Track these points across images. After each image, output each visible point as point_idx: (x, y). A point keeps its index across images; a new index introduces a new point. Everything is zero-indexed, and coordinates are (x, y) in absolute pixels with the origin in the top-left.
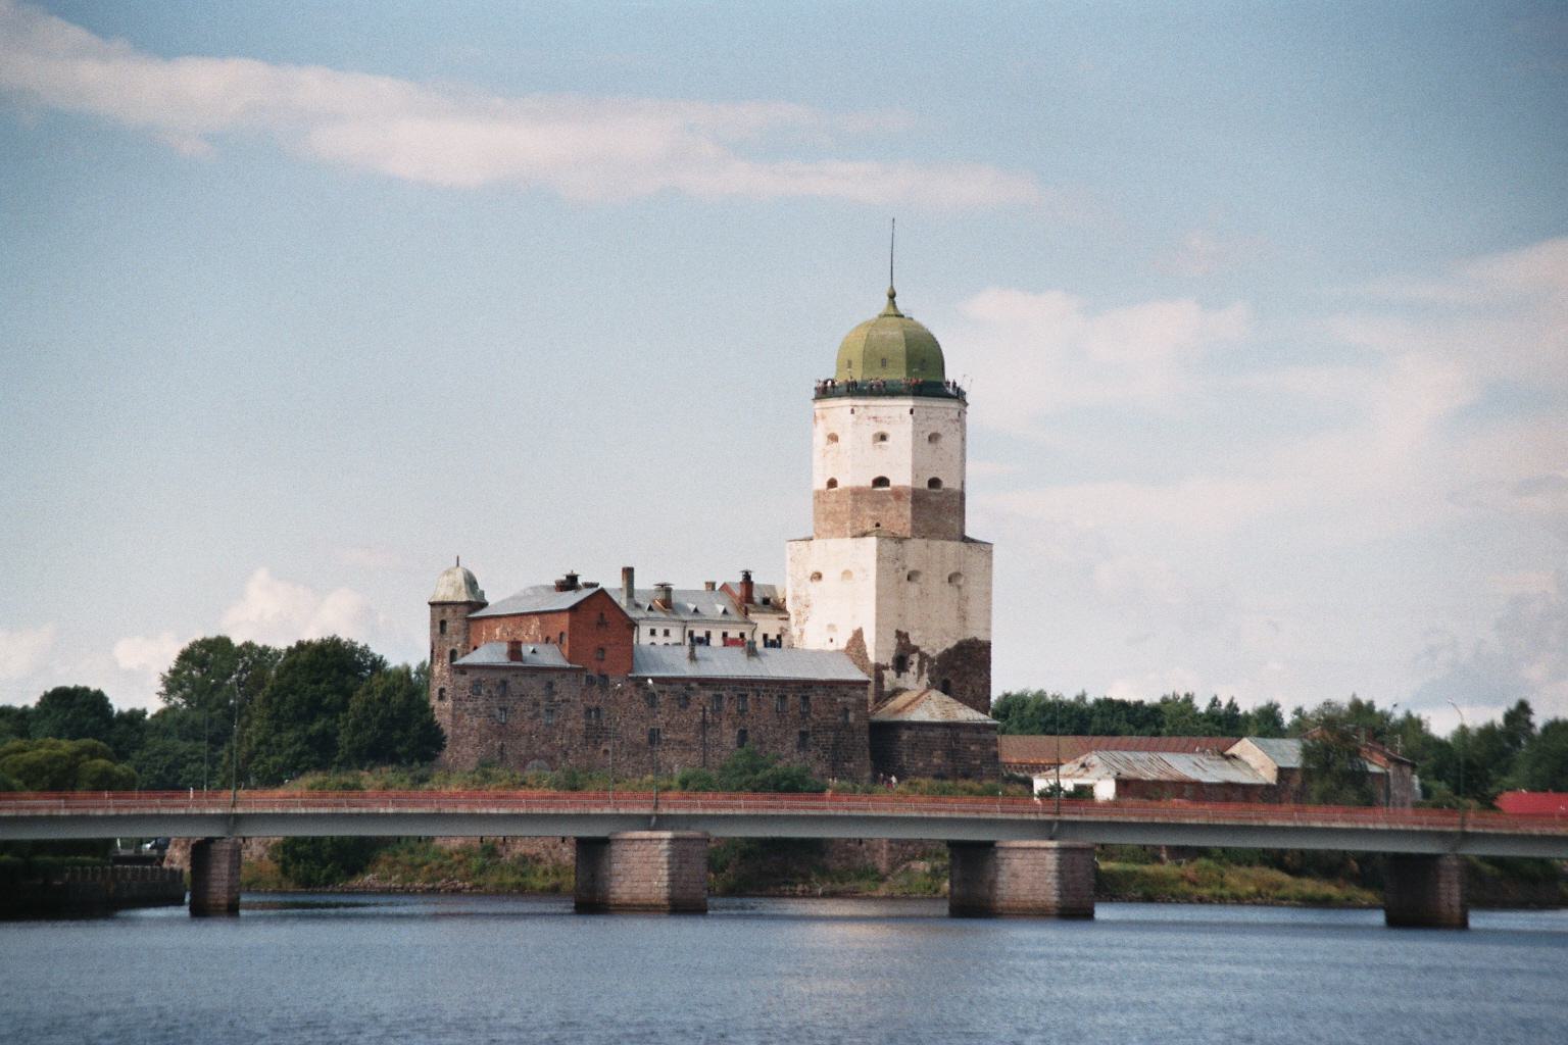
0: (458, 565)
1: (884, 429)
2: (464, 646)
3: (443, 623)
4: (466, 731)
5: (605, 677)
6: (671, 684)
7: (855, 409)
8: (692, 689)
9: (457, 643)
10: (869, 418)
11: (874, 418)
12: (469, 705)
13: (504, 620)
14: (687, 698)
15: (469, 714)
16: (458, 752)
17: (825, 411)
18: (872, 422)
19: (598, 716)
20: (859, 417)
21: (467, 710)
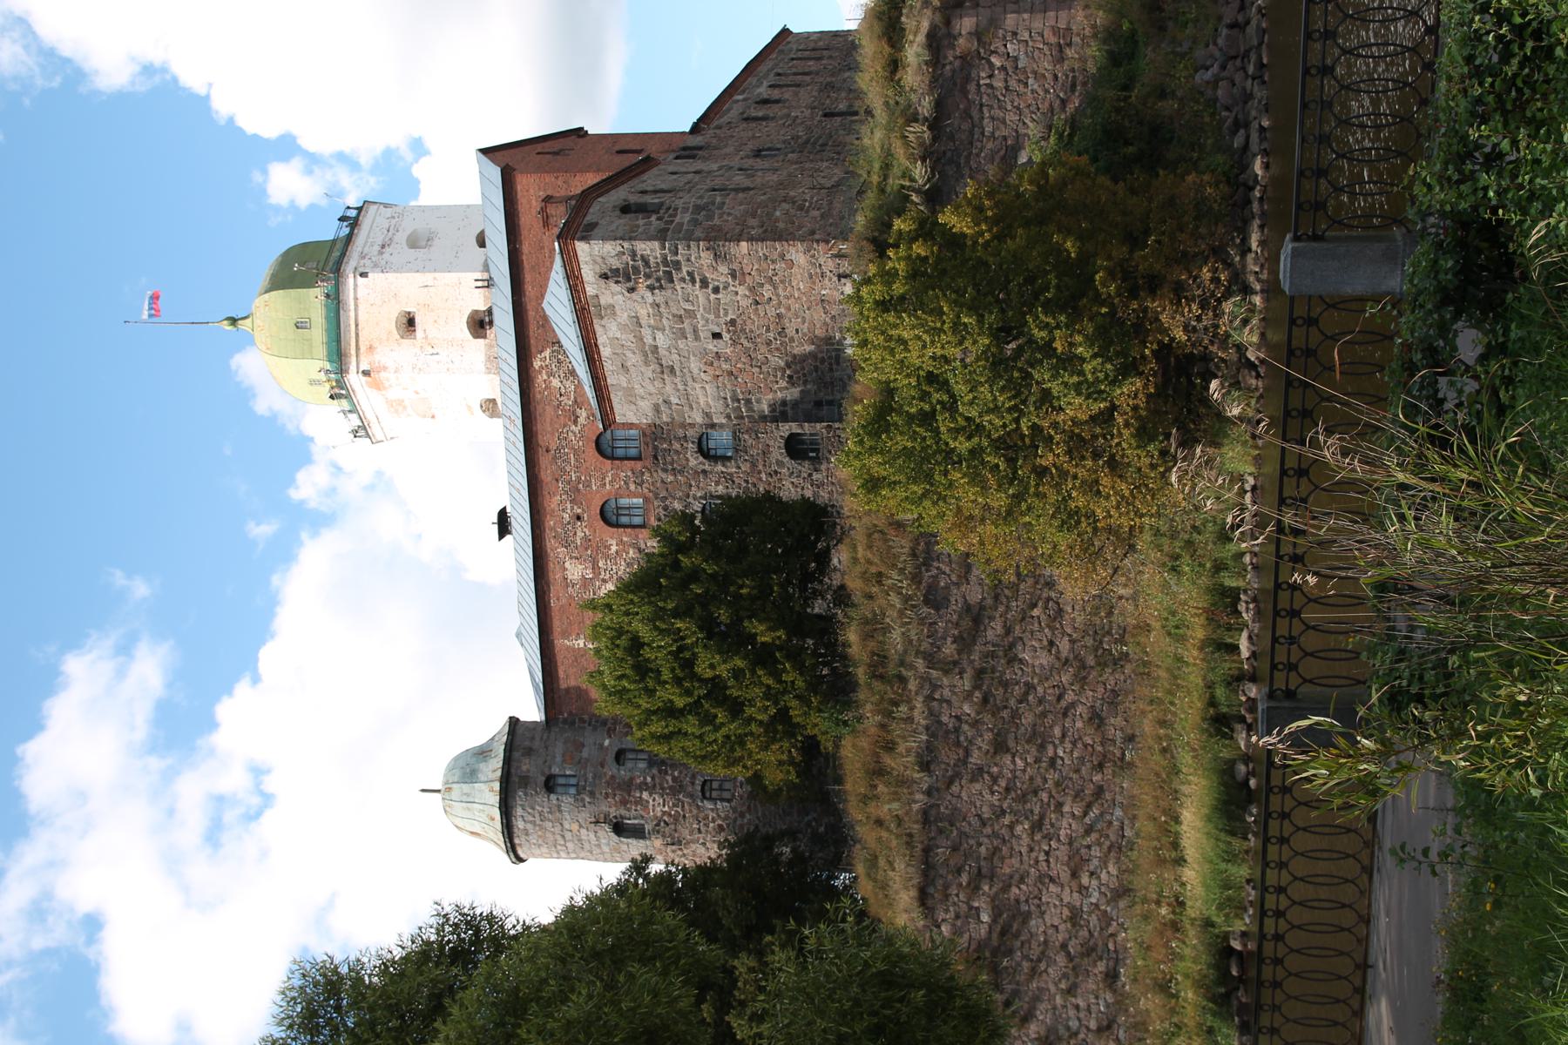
0: (439, 791)
1: (401, 237)
2: (610, 733)
3: (550, 785)
4: (752, 222)
5: (684, 149)
6: (729, 110)
7: (361, 270)
8: (745, 100)
9: (601, 745)
10: (381, 253)
11: (383, 247)
12: (684, 218)
13: (550, 542)
14: (765, 102)
15: (710, 217)
16: (813, 233)
17: (363, 349)
18: (387, 250)
19: (778, 149)
20: (376, 266)
21: (695, 222)
